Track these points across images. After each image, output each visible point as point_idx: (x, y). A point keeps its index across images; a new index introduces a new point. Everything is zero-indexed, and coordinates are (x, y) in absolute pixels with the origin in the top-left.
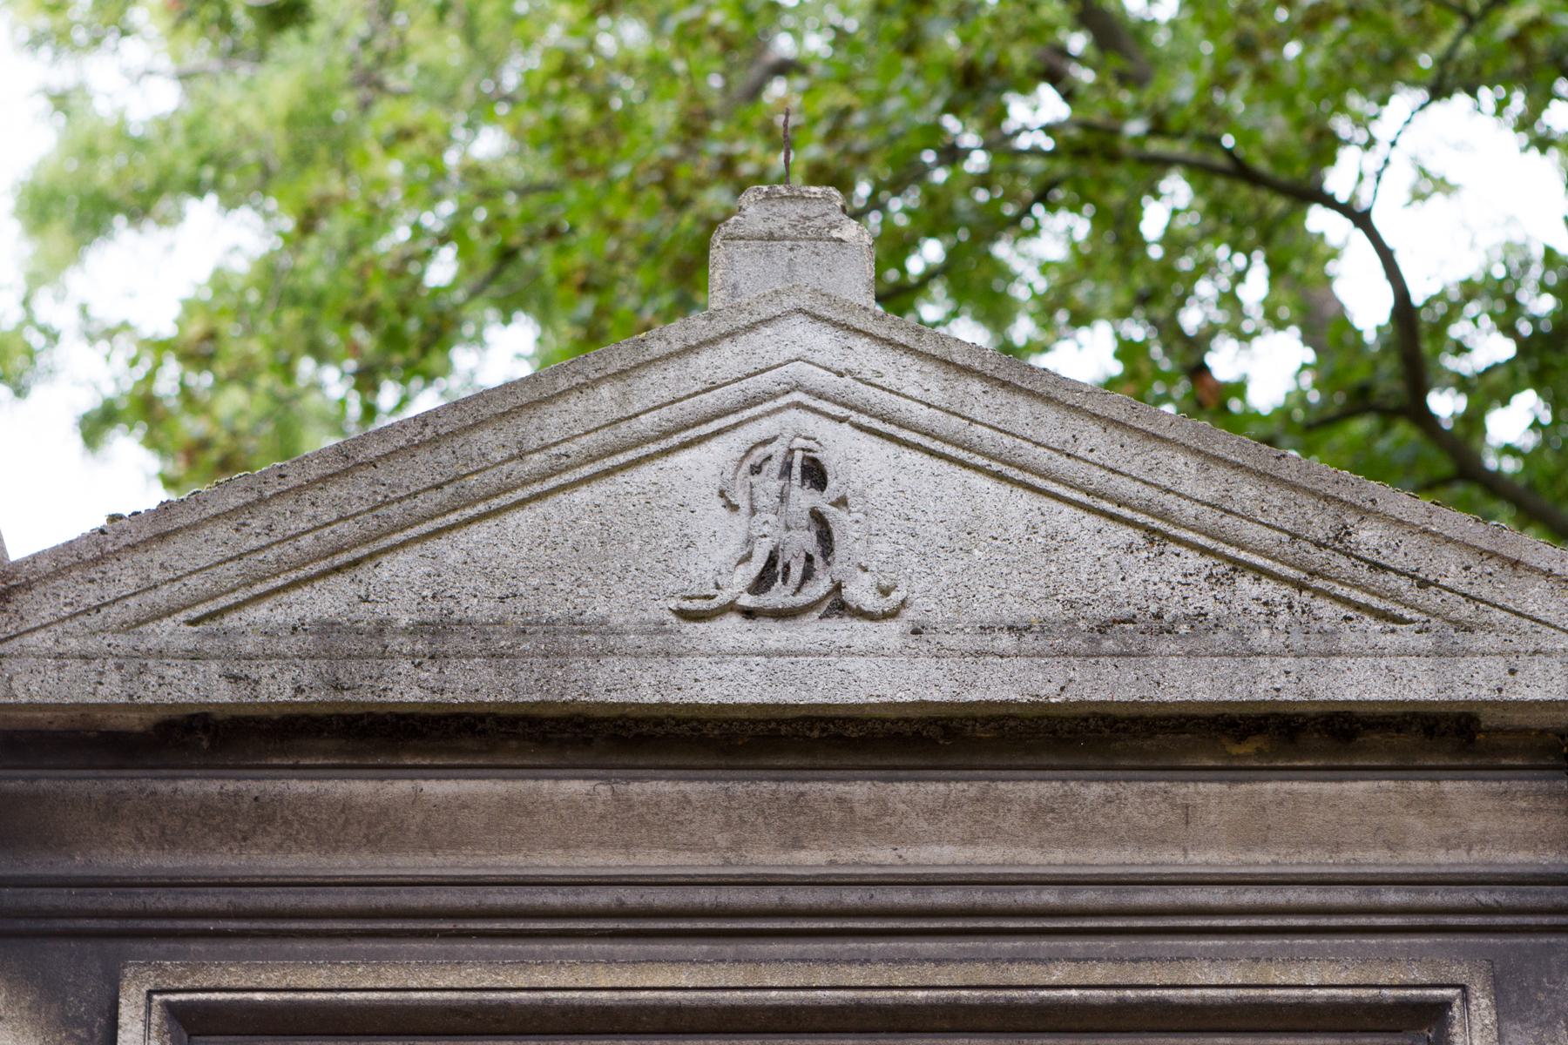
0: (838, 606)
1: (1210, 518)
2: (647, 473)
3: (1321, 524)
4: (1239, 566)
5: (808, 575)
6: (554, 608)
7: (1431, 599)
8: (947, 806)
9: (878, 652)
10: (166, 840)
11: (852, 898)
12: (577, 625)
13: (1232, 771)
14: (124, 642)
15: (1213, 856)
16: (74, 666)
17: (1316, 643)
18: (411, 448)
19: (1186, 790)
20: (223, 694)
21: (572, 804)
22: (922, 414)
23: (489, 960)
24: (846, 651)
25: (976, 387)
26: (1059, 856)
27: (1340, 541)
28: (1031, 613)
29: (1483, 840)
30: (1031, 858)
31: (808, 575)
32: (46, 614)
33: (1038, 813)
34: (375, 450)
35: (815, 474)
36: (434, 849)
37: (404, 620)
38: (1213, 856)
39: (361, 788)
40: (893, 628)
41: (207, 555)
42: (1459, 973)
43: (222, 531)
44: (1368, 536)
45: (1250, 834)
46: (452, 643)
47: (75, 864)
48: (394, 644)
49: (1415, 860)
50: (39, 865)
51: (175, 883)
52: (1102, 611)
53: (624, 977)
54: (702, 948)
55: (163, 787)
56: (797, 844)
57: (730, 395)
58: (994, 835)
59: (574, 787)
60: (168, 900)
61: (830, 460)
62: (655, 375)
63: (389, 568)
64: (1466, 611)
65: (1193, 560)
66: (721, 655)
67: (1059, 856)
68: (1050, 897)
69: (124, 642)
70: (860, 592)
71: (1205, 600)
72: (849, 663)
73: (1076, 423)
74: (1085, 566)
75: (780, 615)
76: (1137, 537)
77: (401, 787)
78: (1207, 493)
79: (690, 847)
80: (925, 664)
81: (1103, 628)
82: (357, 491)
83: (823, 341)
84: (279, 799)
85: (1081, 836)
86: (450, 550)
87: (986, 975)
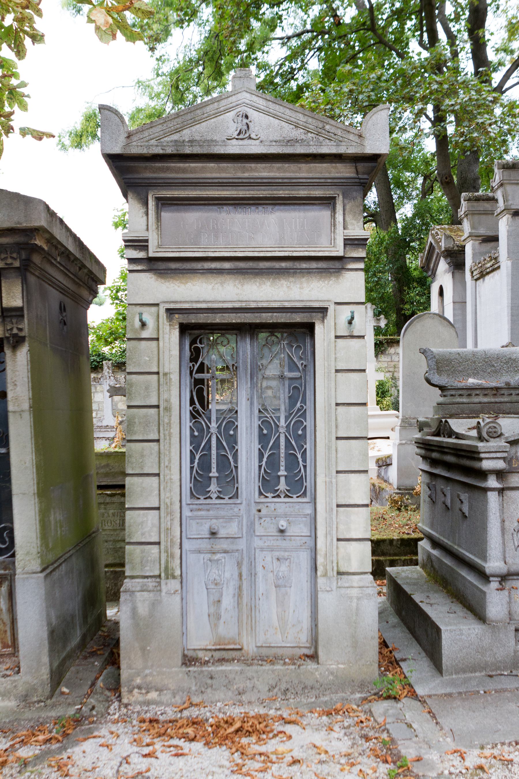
0: (250, 138)
1: (304, 124)
2: (222, 117)
3: (321, 125)
4: (308, 132)
5: (246, 133)
6: (209, 138)
7: (336, 137)
8: (266, 167)
9: (255, 145)
10: (154, 172)
11: (252, 181)
12: (212, 141)
13: (307, 162)
14: (146, 144)
15: (304, 174)
16: (140, 147)
17: (319, 144)
18: (187, 113)
19: (300, 165)
20: (161, 152)
21: (212, 167)
22: (262, 107)
23: (200, 190)
24: (251, 145)
25: (271, 103)
26: (282, 174)
27: (323, 128)
28: (278, 139)
29: (342, 172)
30: (277, 175)
31: (246, 133)
32: (135, 139)
33: (278, 169)
34: (182, 113)
35: (247, 117)
36: (192, 173)
37: (187, 140)
38: (304, 174)
39: (181, 165)
40: (258, 141)
41: (158, 130)
42: (338, 192)
43: (160, 126)
44: (327, 127)
45: (308, 172)
46: (194, 144)
47: (141, 176)
48: (186, 144)
49: (333, 175)
50: (136, 176)
51: (155, 178)
52: (288, 139)
53: (219, 193)
54: (231, 188)
55: (153, 165)
56: (244, 173)
57: (234, 104)
58: (272, 171)
59: (212, 165)
60: (155, 181)
61: (249, 115)
62: (223, 101)
63: (185, 132)
64: (341, 139)
65: (302, 131)
66: (233, 146)
67: (282, 174)
68: (280, 181)
69: (146, 144)
70: (253, 136)
71: (303, 137)
72: (251, 147)
73: (285, 109)
74: (286, 131)
75: (242, 139)
76: (294, 127)
77: (187, 165)
78: (304, 120)
79: (229, 173)
80: (262, 147)
81: (288, 141)
82: (179, 120)
83: (248, 95)
84: (170, 167)
85: (285, 172)
86: (194, 129)
87: (271, 192)
